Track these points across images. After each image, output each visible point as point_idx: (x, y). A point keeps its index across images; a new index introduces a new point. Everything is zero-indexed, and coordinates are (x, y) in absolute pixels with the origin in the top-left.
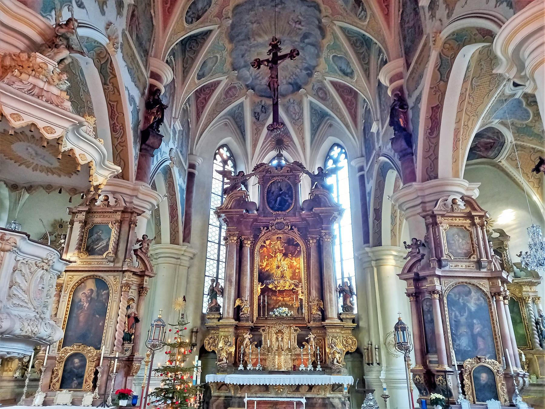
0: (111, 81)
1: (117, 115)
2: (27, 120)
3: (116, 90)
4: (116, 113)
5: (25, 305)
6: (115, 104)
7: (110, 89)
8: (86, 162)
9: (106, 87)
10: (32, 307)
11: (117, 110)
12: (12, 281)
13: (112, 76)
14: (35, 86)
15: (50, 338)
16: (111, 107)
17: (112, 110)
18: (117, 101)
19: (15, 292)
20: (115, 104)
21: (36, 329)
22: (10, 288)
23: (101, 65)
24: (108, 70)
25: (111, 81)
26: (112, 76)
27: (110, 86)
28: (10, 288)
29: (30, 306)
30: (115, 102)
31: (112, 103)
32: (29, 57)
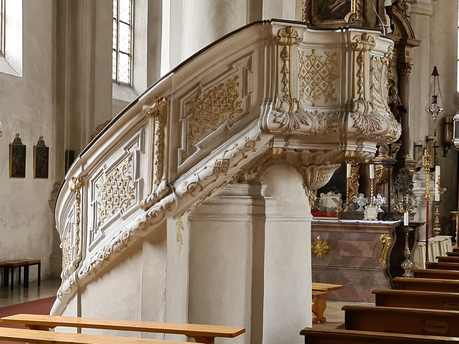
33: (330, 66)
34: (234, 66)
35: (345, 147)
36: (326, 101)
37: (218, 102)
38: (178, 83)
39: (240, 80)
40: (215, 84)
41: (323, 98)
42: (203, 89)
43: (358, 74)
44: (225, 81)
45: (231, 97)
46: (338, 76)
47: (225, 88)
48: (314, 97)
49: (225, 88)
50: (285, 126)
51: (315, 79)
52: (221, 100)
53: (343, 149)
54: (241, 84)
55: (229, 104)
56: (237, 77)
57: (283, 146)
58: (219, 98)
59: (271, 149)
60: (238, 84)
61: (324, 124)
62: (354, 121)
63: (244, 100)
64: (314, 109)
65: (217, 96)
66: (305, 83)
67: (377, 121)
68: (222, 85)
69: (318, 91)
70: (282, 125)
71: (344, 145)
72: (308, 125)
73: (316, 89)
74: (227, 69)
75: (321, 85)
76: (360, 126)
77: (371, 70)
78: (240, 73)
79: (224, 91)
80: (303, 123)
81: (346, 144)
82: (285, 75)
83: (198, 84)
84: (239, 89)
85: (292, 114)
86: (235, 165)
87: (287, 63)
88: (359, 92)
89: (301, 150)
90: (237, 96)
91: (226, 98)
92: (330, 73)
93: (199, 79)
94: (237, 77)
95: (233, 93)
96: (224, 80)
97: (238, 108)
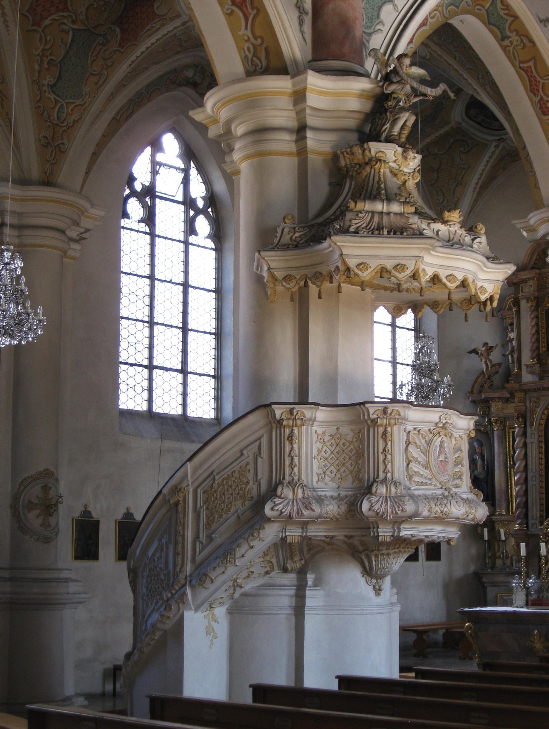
0: (512, 28)
1: (542, 81)
2: (374, 264)
3: (525, 41)
4: (538, 79)
5: (429, 482)
6: (531, 64)
7: (515, 43)
8: (457, 283)
9: (506, 42)
10: (438, 484)
11: (538, 75)
12: (407, 458)
13: (510, 19)
14: (373, 213)
15: (471, 517)
16: (526, 72)
17: (530, 77)
18: (534, 58)
19: (415, 469)
20: (531, 64)
21: (446, 509)
22: (408, 465)
23: (487, 11)
24: (502, 13)
25: (512, 28)
26: (510, 19)
27: (514, 38)
28: (408, 465)
29: (434, 482)
30: (529, 61)
31: (525, 65)
32: (364, 150)
33: (356, 444)
34: (245, 452)
35: (378, 533)
36: (353, 482)
37: (230, 490)
38: (195, 470)
39: (251, 467)
40: (228, 471)
41: (350, 479)
42: (217, 478)
43: (383, 451)
44: (237, 468)
45: (243, 484)
46: (363, 455)
47: (236, 474)
48: (341, 478)
49: (236, 474)
50: (285, 514)
51: (341, 458)
52: (233, 488)
53: (376, 534)
54: (252, 471)
55: (241, 492)
56: (247, 464)
57: (300, 534)
58: (231, 486)
59: (286, 537)
60: (249, 470)
61: (343, 508)
62: (370, 504)
63: (255, 487)
64: (337, 492)
65: (230, 484)
66: (328, 465)
67: (400, 503)
68: (234, 472)
69: (345, 471)
70: (282, 513)
71: (375, 530)
72: (313, 511)
73: (342, 470)
74: (239, 454)
75: (348, 464)
76: (378, 509)
77: (408, 443)
78: (251, 459)
79: (236, 478)
80: (308, 509)
81: (378, 528)
82: (292, 459)
83: (212, 473)
84: (250, 476)
85: (296, 500)
86: (243, 556)
87: (296, 446)
88: (384, 471)
89: (332, 537)
90: (248, 483)
91: (237, 486)
92: (357, 451)
93: (214, 467)
94: (247, 464)
95: (244, 480)
96: (236, 467)
97: (249, 496)
